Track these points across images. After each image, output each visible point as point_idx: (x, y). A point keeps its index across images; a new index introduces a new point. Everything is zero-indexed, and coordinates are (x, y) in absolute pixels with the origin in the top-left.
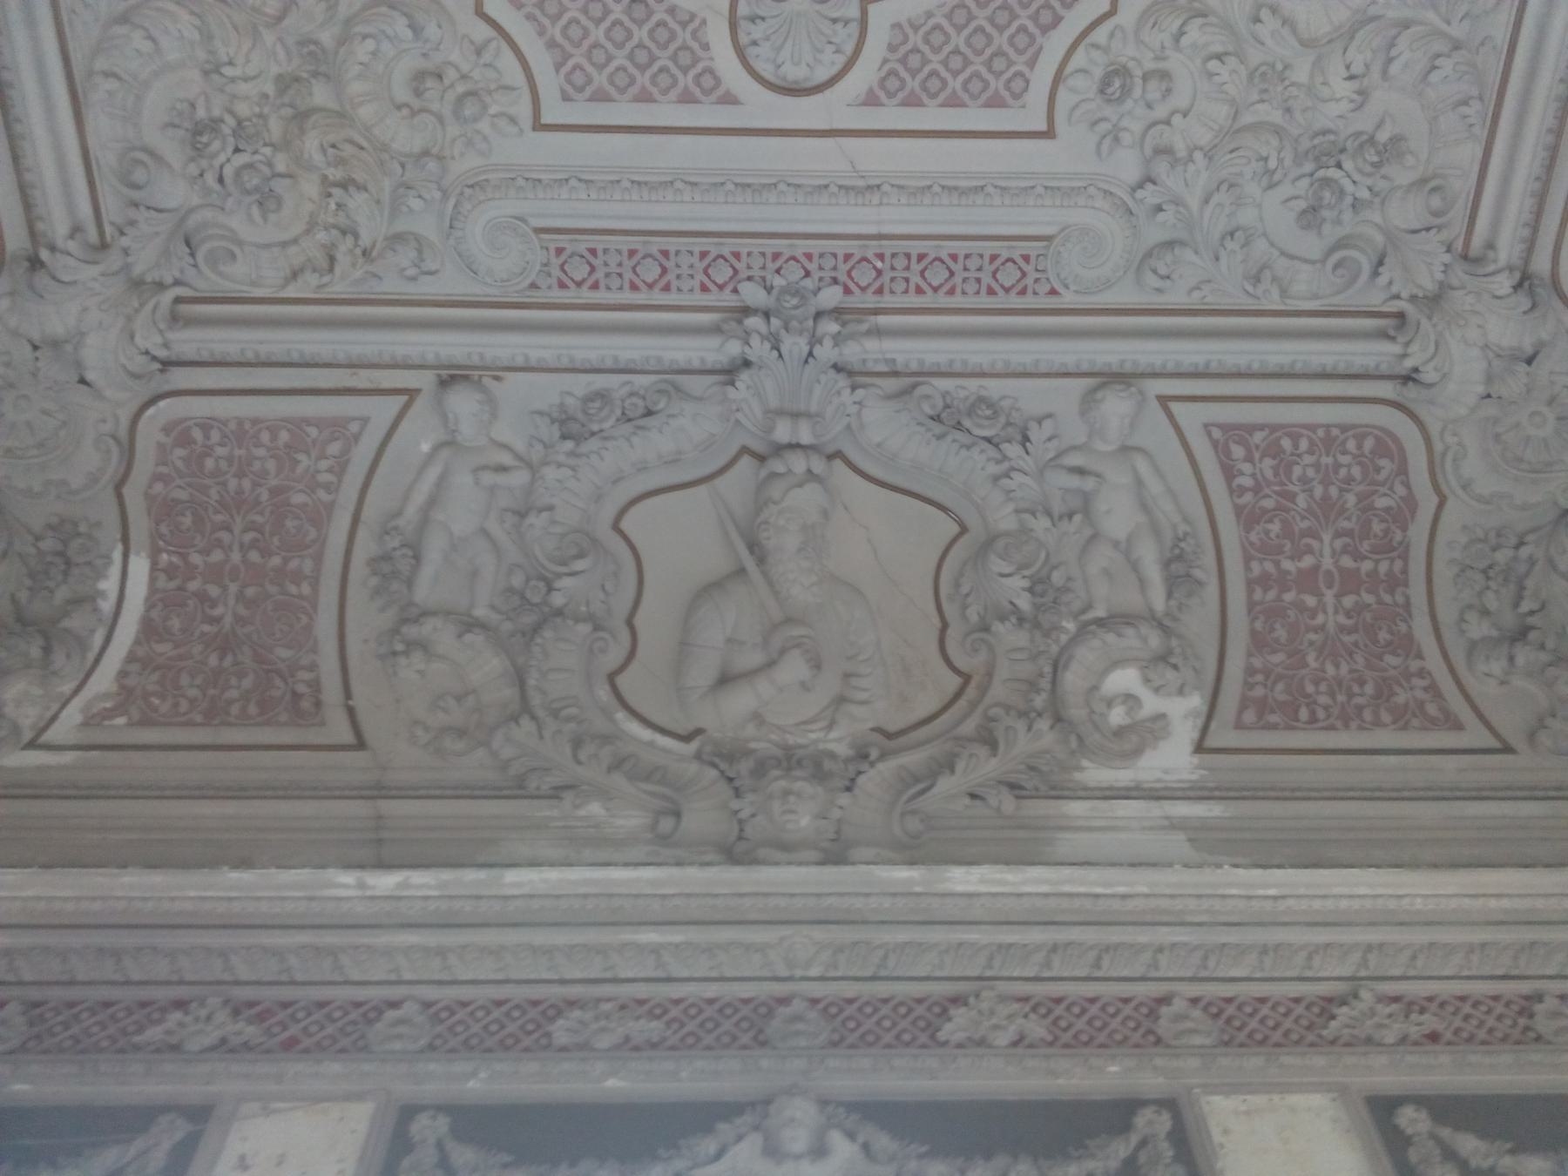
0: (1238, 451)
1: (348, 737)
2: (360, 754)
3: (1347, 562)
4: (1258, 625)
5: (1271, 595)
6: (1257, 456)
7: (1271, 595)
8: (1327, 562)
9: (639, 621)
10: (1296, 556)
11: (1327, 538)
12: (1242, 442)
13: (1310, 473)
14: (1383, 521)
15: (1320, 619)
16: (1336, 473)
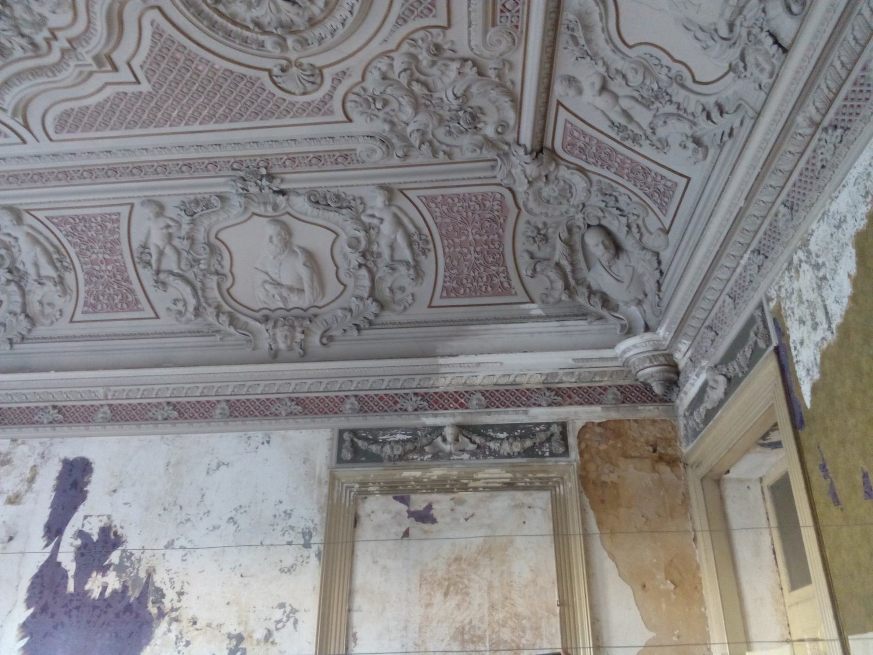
0: (433, 205)
1: (153, 315)
2: (158, 320)
3: (477, 237)
4: (448, 261)
5: (452, 250)
6: (440, 206)
7: (452, 250)
8: (471, 238)
9: (234, 270)
10: (459, 237)
11: (470, 230)
12: (433, 202)
13: (461, 209)
14: (489, 221)
15: (469, 256)
16: (469, 208)
